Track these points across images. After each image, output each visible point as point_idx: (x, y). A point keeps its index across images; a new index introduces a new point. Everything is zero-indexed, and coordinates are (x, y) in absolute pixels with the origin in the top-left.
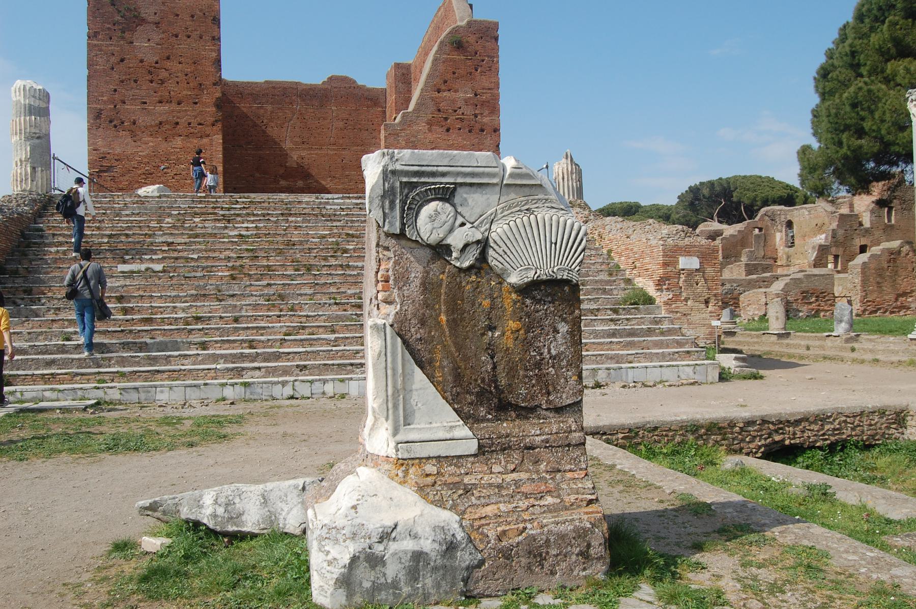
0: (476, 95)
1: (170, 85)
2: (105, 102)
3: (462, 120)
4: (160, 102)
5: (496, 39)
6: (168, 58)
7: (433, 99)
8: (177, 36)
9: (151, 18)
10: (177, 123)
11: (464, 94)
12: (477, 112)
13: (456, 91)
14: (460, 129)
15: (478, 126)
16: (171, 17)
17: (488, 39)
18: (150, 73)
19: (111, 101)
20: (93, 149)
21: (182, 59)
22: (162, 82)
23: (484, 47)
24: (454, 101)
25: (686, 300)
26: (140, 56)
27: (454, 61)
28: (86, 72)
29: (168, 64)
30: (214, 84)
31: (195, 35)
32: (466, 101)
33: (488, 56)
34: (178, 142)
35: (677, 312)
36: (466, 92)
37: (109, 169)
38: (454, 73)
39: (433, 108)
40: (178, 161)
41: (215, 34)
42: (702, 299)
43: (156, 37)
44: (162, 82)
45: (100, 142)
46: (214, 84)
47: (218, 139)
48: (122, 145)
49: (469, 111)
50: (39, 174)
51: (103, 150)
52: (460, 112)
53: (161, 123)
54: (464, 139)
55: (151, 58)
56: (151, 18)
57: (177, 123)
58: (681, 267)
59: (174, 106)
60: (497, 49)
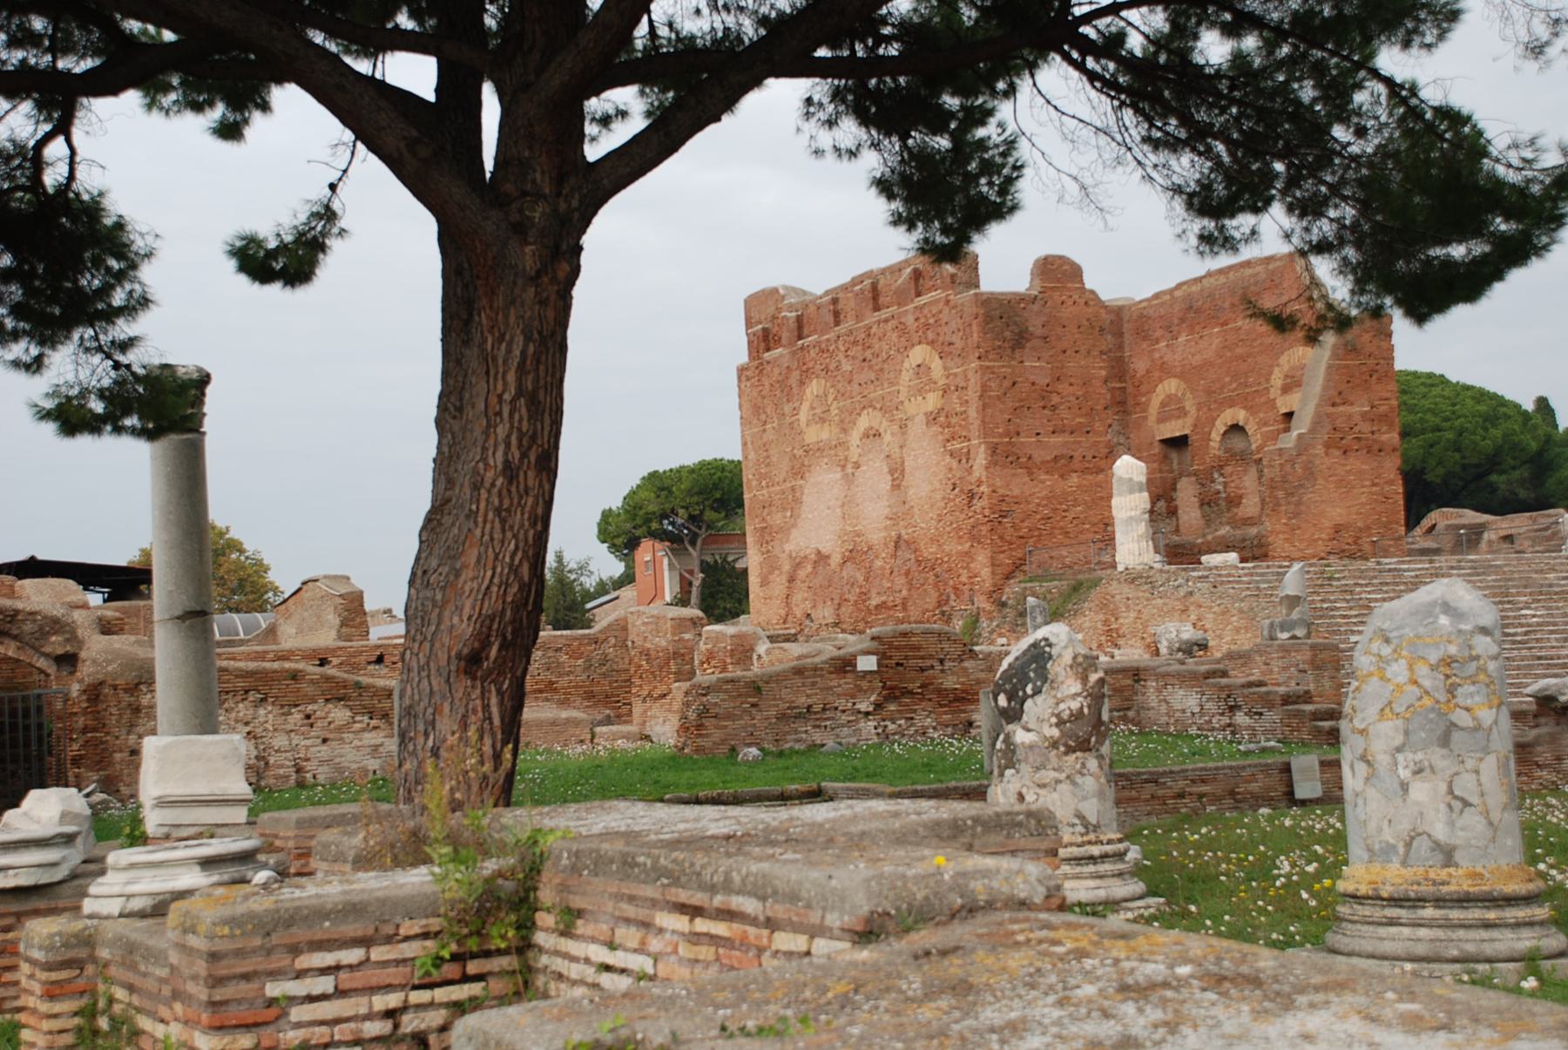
2: (1001, 436)
5: (1390, 335)
7: (1328, 415)
9: (1039, 332)
11: (1360, 408)
15: (1376, 447)
16: (1059, 330)
19: (1007, 434)
22: (1054, 408)
24: (1350, 417)
26: (1032, 378)
31: (1083, 349)
32: (1364, 415)
34: (1074, 479)
39: (1329, 427)
40: (1076, 503)
43: (1046, 355)
44: (1054, 408)
45: (998, 482)
48: (1018, 485)
49: (1365, 427)
51: (1001, 491)
52: (1356, 429)
56: (1039, 332)
60: (1391, 348)
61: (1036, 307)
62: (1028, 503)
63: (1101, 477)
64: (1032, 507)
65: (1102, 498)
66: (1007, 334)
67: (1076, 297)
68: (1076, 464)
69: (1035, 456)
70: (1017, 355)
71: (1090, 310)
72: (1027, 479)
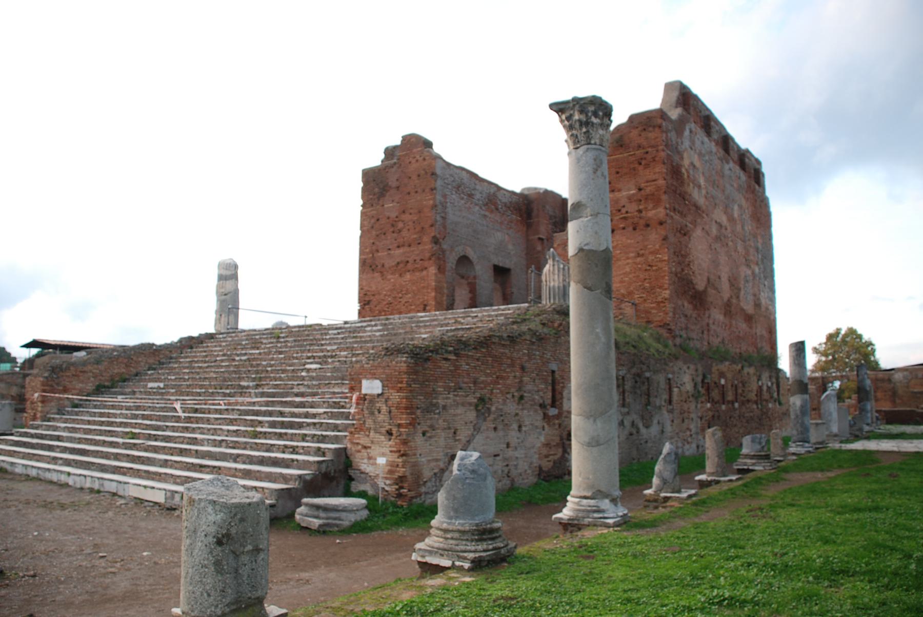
0: (640, 190)
1: (405, 233)
2: (368, 253)
3: (625, 218)
4: (398, 247)
6: (404, 212)
8: (409, 193)
10: (408, 262)
12: (641, 207)
13: (619, 190)
14: (624, 228)
15: (642, 222)
17: (651, 129)
18: (393, 226)
19: (372, 252)
20: (361, 288)
21: (411, 211)
22: (400, 231)
23: (647, 138)
25: (369, 429)
26: (387, 214)
27: (617, 160)
28: (359, 232)
29: (404, 217)
30: (432, 226)
32: (630, 199)
33: (652, 147)
34: (408, 276)
35: (358, 444)
36: (629, 190)
37: (368, 303)
38: (618, 173)
41: (433, 186)
42: (383, 430)
45: (364, 284)
46: (432, 226)
47: (433, 270)
49: (632, 208)
50: (223, 319)
51: (366, 288)
52: (623, 210)
53: (398, 263)
54: (627, 238)
55: (393, 215)
57: (408, 262)
58: (364, 391)
59: (406, 249)
61: (395, 168)
62: (379, 294)
63: (425, 273)
64: (382, 297)
65: (424, 287)
66: (377, 190)
67: (418, 157)
68: (410, 266)
69: (387, 266)
70: (381, 202)
71: (426, 163)
72: (380, 279)
